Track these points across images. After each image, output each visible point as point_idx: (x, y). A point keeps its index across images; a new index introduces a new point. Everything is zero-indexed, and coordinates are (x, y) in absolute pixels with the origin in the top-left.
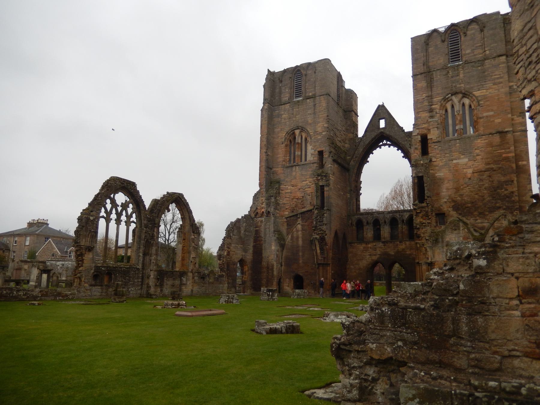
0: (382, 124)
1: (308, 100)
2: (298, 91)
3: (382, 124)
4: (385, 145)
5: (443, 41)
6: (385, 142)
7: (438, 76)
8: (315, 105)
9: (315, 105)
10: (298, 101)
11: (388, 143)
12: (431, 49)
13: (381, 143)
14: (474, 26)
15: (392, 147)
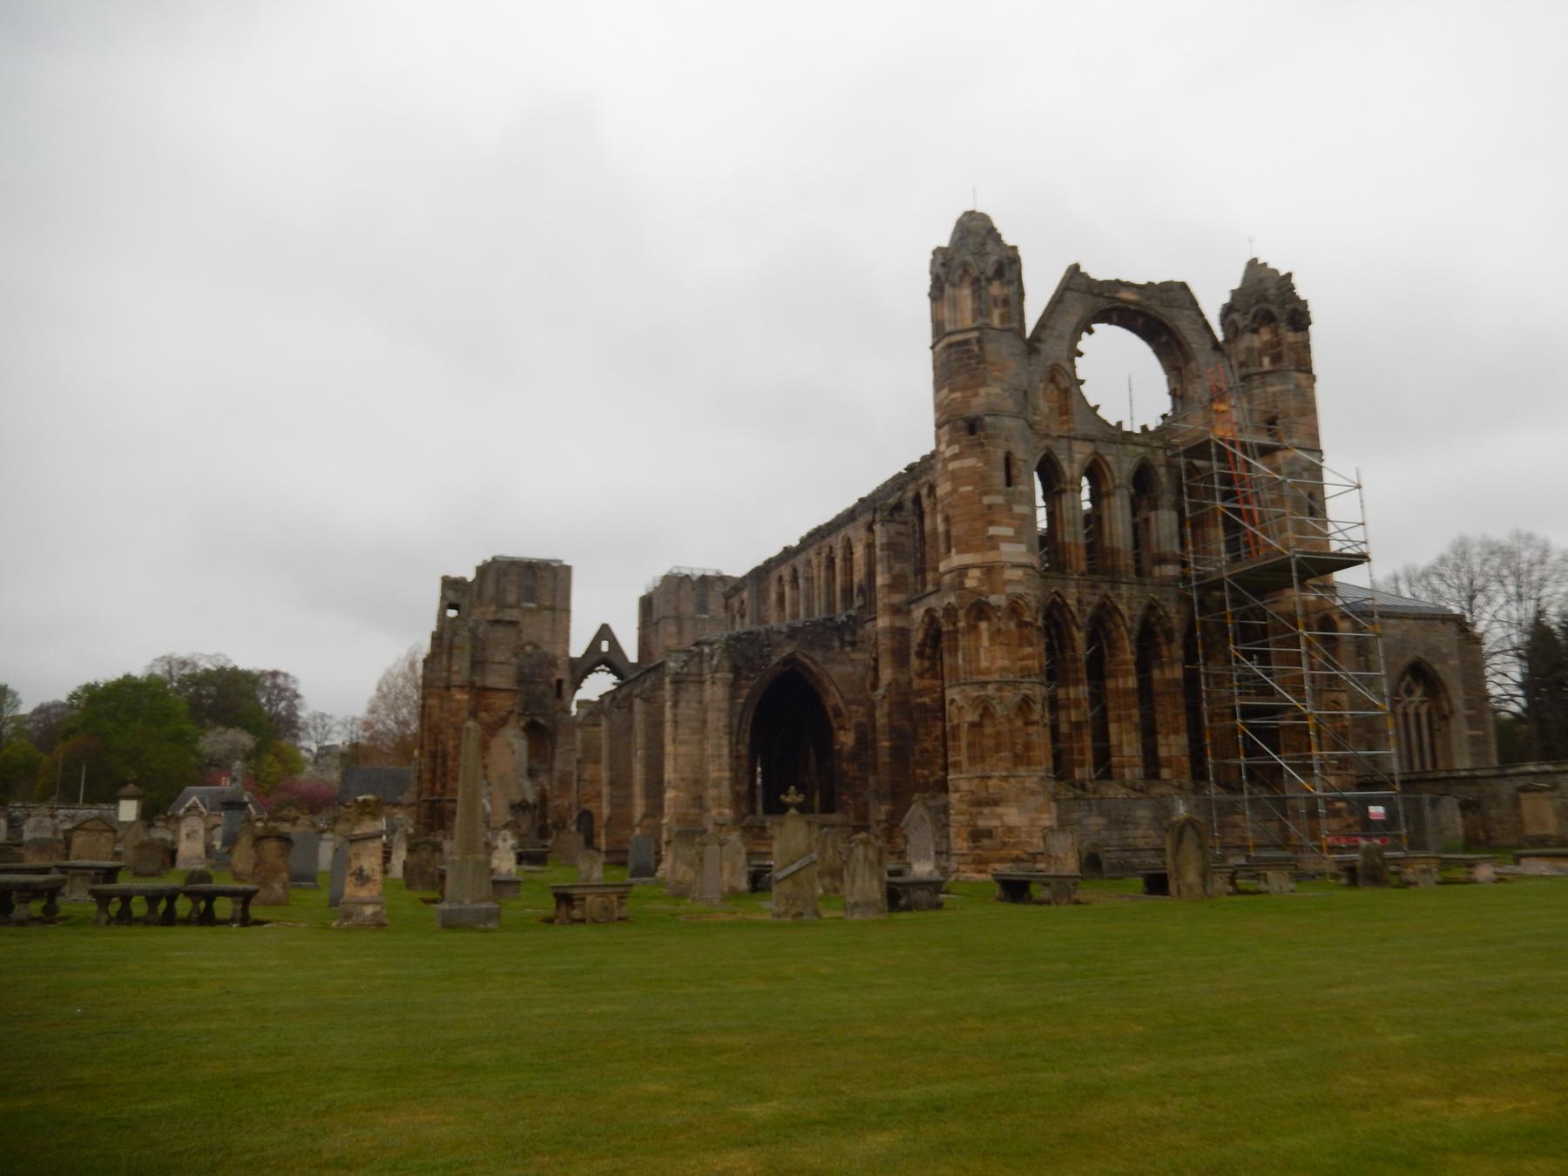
0: (605, 646)
1: (545, 612)
2: (530, 594)
3: (605, 646)
4: (603, 671)
5: (693, 589)
6: (603, 667)
7: (688, 626)
8: (554, 620)
9: (554, 620)
10: (531, 610)
11: (608, 669)
12: (682, 593)
13: (598, 668)
14: (720, 584)
15: (611, 675)
